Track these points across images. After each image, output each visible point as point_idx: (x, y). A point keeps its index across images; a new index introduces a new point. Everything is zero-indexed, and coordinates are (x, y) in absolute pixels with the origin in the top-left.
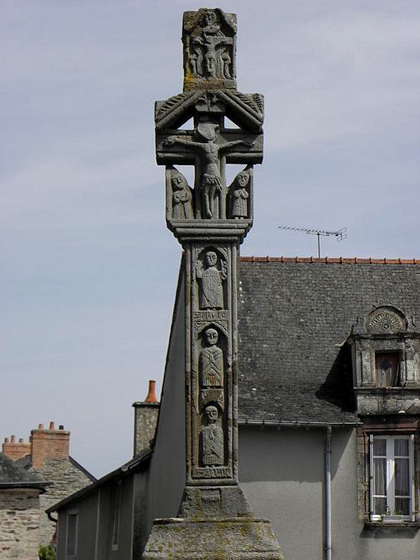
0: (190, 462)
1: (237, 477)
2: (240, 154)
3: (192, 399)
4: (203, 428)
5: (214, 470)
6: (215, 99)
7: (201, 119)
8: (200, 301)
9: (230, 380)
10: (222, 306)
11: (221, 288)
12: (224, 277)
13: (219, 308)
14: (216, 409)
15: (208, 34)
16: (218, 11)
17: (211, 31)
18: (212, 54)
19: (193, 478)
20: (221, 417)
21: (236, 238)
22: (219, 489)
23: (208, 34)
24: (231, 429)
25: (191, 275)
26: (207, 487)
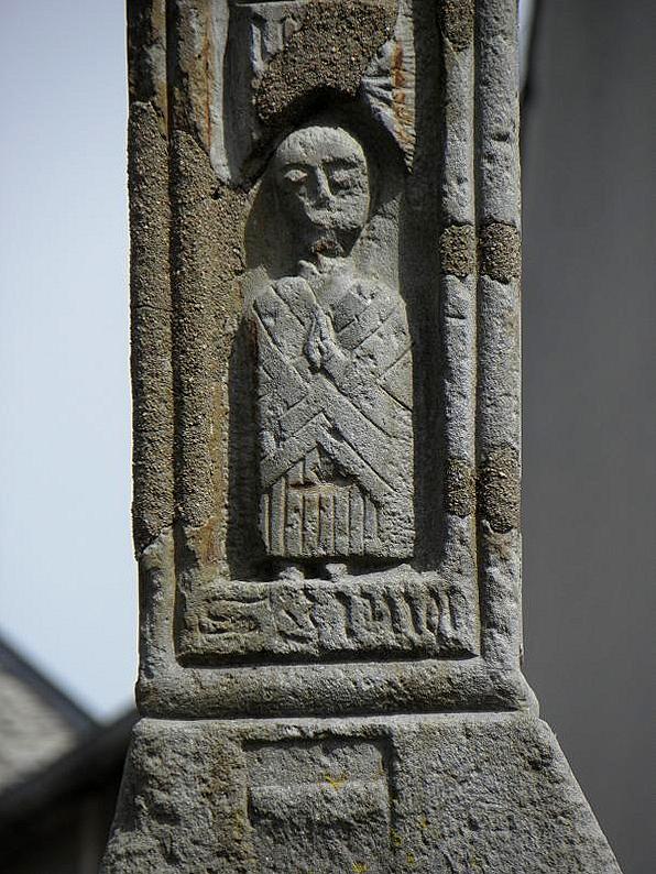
0: (168, 537)
1: (511, 646)
4: (265, 286)
5: (342, 597)
14: (349, 145)
19: (189, 660)
20: (392, 206)
22: (382, 739)
24: (463, 293)
26: (292, 726)
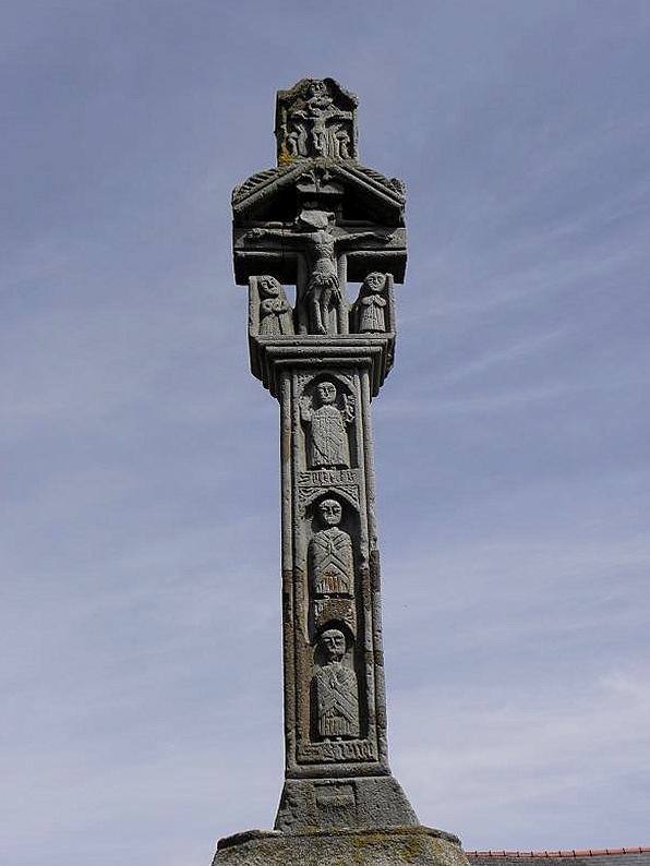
0: (294, 731)
2: (369, 252)
3: (296, 617)
4: (318, 668)
6: (327, 176)
7: (307, 204)
8: (308, 459)
9: (367, 582)
10: (348, 464)
11: (344, 435)
12: (350, 418)
13: (341, 467)
15: (314, 106)
16: (329, 83)
17: (319, 103)
18: (321, 128)
19: (299, 763)
20: (351, 650)
21: (369, 359)
22: (353, 784)
23: (314, 106)
24: (370, 668)
25: (293, 418)
26: (328, 781)
